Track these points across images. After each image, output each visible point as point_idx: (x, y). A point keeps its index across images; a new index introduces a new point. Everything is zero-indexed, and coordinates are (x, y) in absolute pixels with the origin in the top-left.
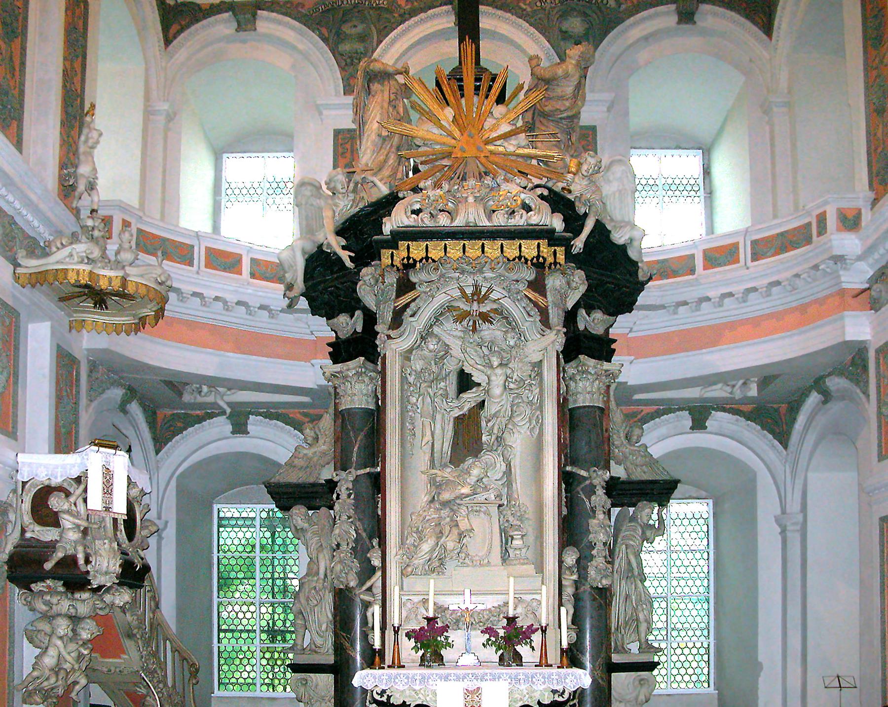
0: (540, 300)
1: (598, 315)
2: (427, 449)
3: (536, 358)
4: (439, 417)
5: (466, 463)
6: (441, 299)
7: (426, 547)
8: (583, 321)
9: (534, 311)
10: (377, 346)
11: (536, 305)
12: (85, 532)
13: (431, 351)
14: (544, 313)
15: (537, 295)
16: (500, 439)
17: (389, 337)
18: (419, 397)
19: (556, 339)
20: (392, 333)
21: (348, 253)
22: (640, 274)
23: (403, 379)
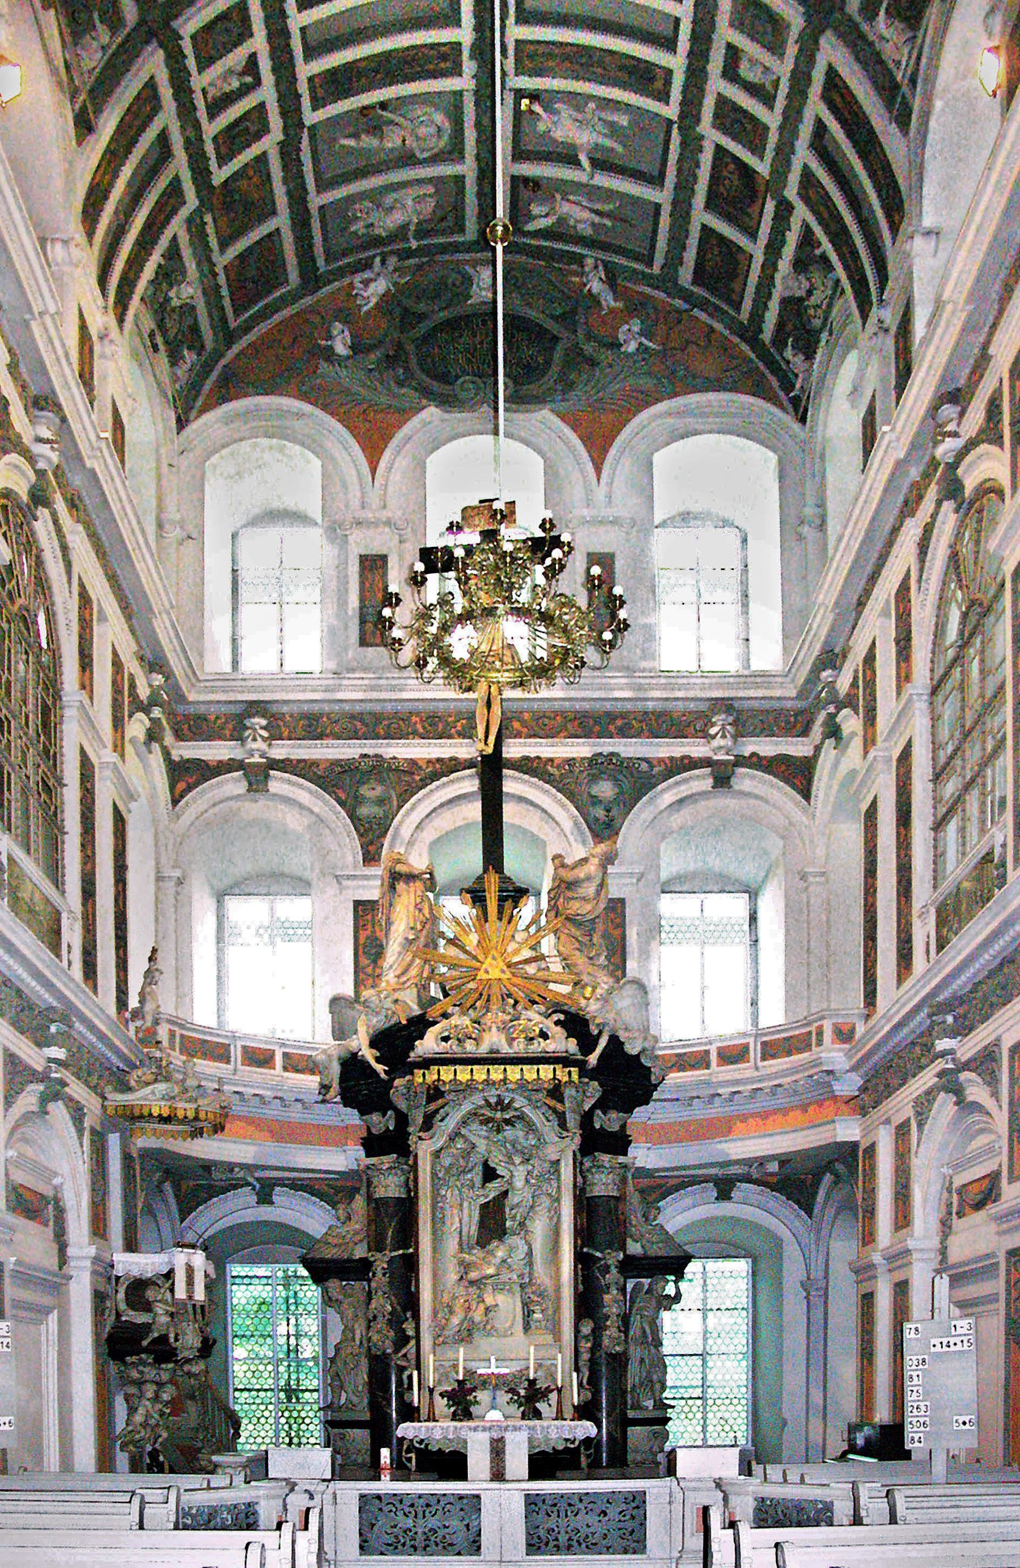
2: (456, 1235)
4: (466, 1204)
6: (467, 1107)
12: (172, 1315)
16: (522, 1224)
17: (420, 1138)
23: (434, 1175)
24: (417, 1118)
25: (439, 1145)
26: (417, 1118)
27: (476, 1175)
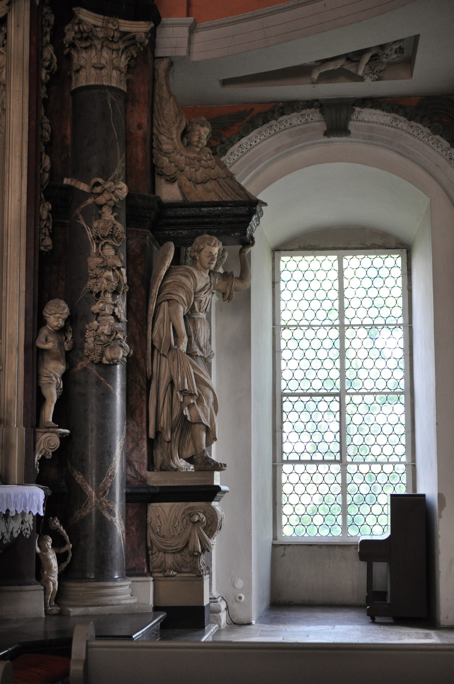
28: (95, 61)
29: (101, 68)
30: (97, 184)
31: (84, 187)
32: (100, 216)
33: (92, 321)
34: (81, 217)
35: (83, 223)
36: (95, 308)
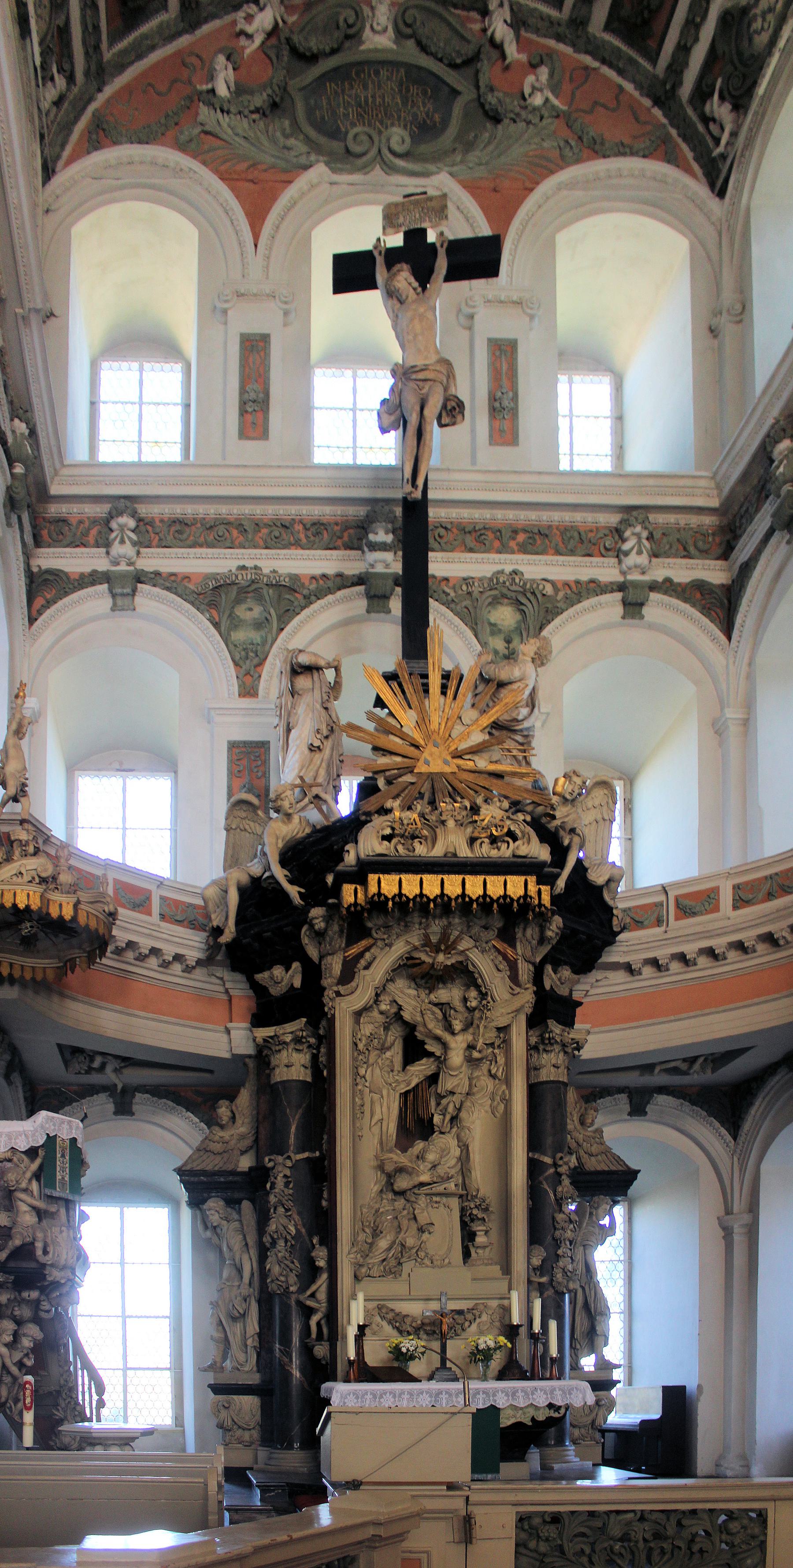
0: (509, 951)
1: (566, 972)
3: (502, 1022)
5: (415, 1148)
7: (383, 1244)
8: (550, 979)
9: (503, 966)
10: (324, 1005)
11: (505, 957)
13: (381, 1013)
14: (513, 966)
15: (506, 946)
16: (454, 1119)
17: (338, 994)
18: (367, 1068)
19: (527, 997)
20: (342, 989)
21: (297, 889)
22: (615, 922)
24: (335, 965)
25: (358, 1006)
26: (335, 965)
27: (396, 1054)
28: (553, 1062)
29: (558, 1068)
30: (561, 1158)
31: (548, 1160)
32: (560, 1182)
33: (558, 1261)
34: (544, 1183)
35: (545, 1186)
36: (560, 1252)
